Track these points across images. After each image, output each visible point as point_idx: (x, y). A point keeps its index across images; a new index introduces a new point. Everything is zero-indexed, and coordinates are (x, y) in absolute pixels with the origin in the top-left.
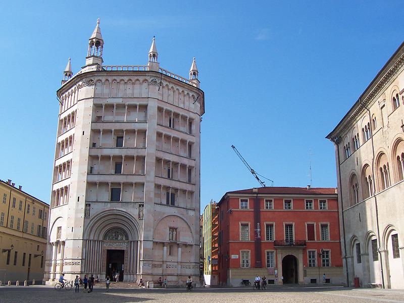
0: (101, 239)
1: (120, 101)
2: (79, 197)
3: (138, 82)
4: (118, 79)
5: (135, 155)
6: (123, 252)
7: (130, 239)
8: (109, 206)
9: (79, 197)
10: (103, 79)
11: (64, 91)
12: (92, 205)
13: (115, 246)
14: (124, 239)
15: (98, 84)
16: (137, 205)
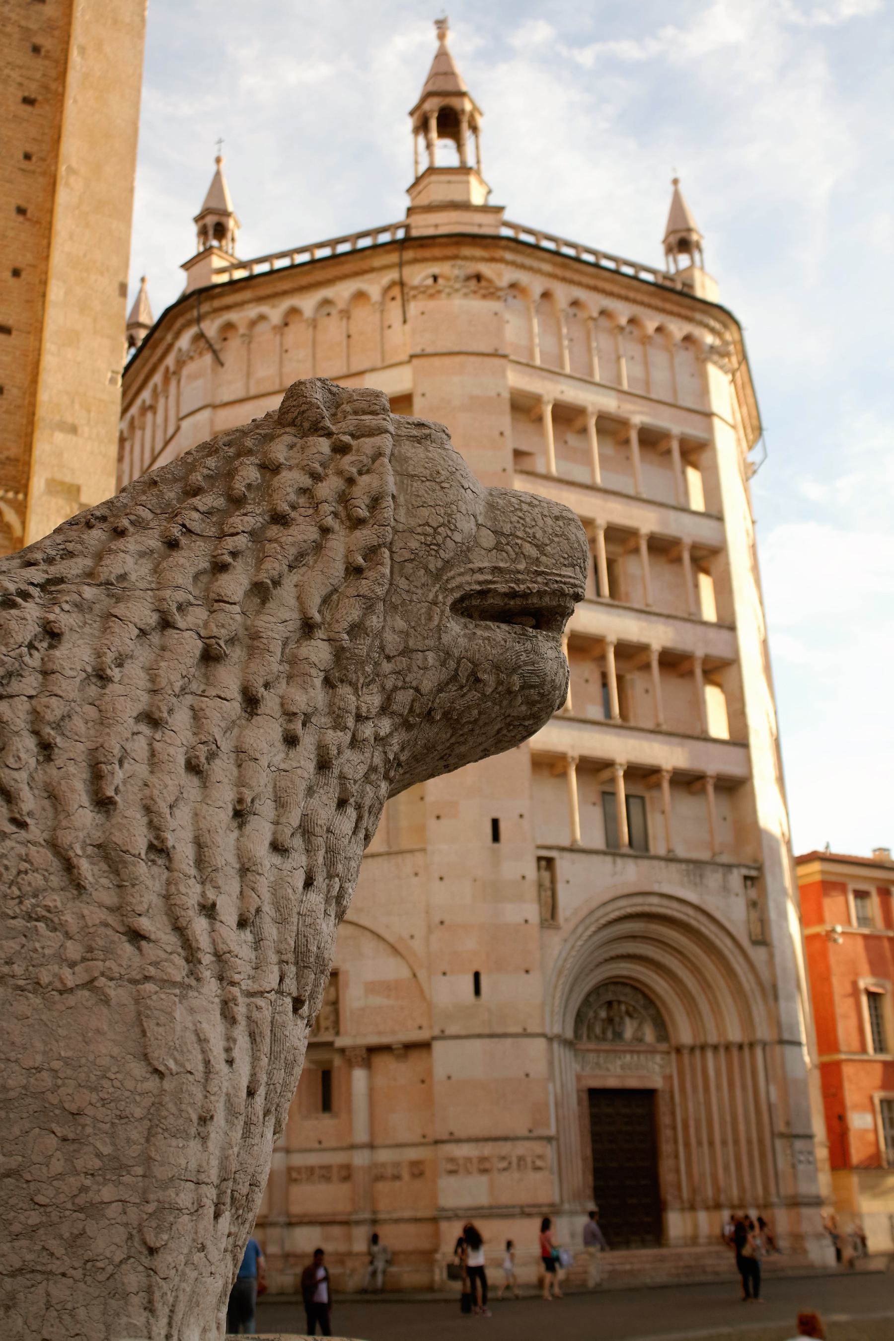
0: (569, 1034)
1: (609, 403)
2: (495, 823)
3: (658, 339)
4: (594, 302)
5: (700, 653)
6: (648, 1095)
7: (685, 1035)
8: (630, 874)
9: (495, 823)
10: (536, 285)
11: (247, 295)
12: (564, 865)
13: (619, 1072)
14: (649, 1035)
15: (510, 299)
16: (735, 879)
